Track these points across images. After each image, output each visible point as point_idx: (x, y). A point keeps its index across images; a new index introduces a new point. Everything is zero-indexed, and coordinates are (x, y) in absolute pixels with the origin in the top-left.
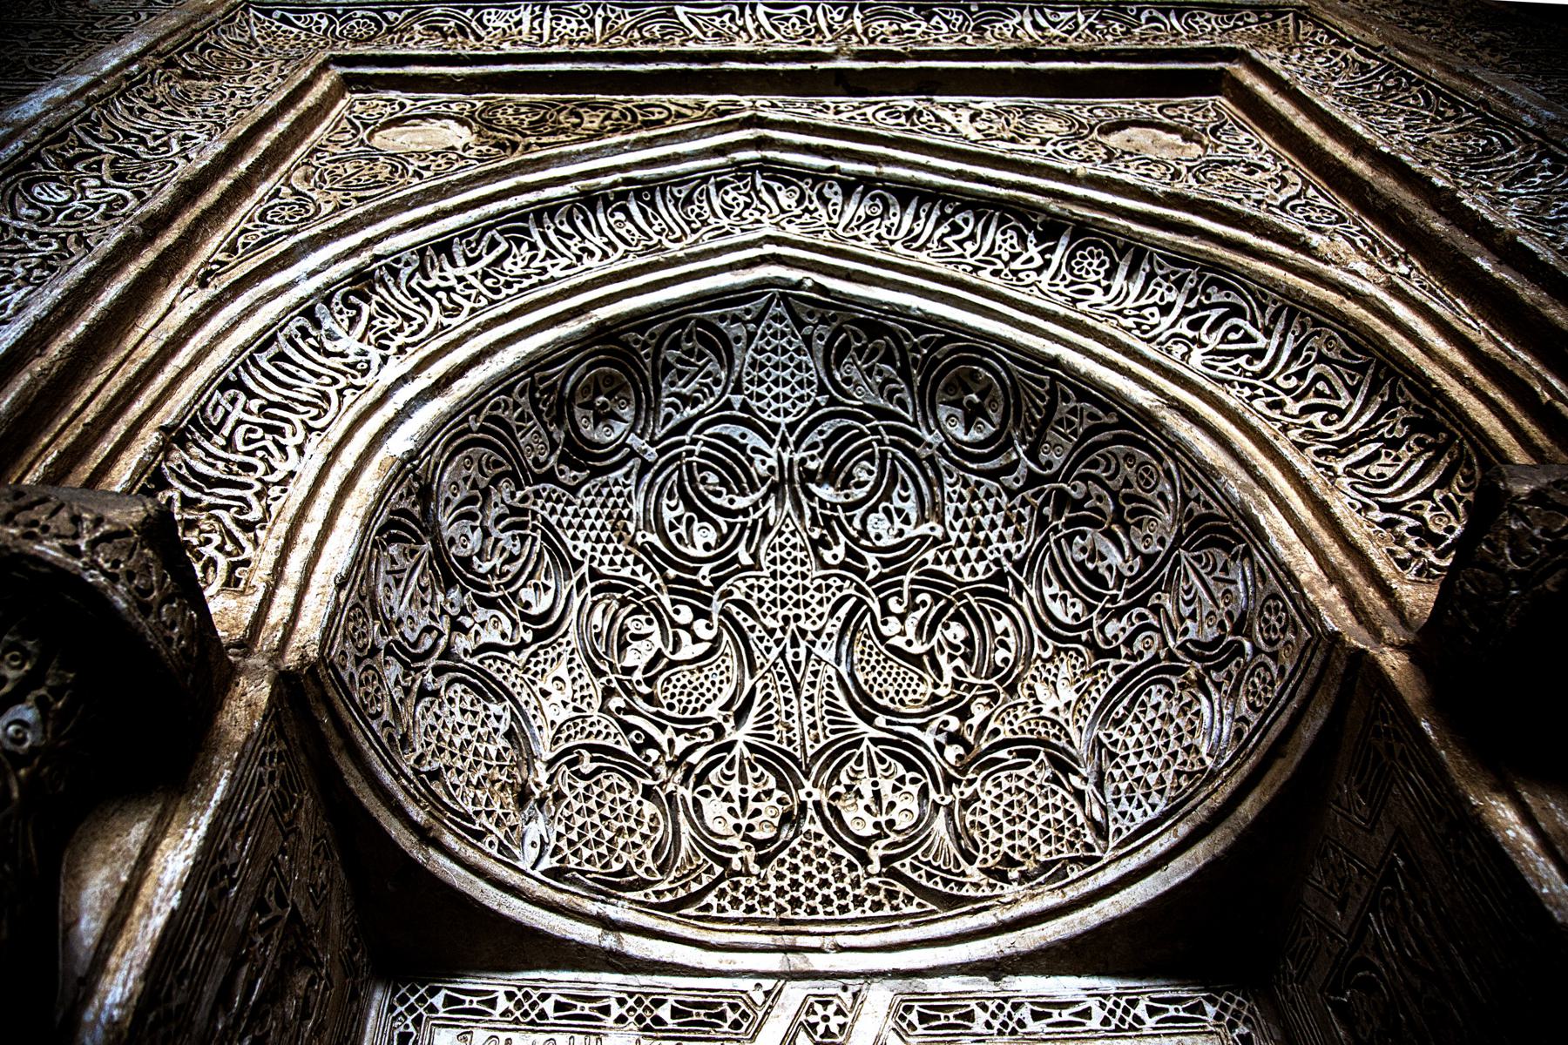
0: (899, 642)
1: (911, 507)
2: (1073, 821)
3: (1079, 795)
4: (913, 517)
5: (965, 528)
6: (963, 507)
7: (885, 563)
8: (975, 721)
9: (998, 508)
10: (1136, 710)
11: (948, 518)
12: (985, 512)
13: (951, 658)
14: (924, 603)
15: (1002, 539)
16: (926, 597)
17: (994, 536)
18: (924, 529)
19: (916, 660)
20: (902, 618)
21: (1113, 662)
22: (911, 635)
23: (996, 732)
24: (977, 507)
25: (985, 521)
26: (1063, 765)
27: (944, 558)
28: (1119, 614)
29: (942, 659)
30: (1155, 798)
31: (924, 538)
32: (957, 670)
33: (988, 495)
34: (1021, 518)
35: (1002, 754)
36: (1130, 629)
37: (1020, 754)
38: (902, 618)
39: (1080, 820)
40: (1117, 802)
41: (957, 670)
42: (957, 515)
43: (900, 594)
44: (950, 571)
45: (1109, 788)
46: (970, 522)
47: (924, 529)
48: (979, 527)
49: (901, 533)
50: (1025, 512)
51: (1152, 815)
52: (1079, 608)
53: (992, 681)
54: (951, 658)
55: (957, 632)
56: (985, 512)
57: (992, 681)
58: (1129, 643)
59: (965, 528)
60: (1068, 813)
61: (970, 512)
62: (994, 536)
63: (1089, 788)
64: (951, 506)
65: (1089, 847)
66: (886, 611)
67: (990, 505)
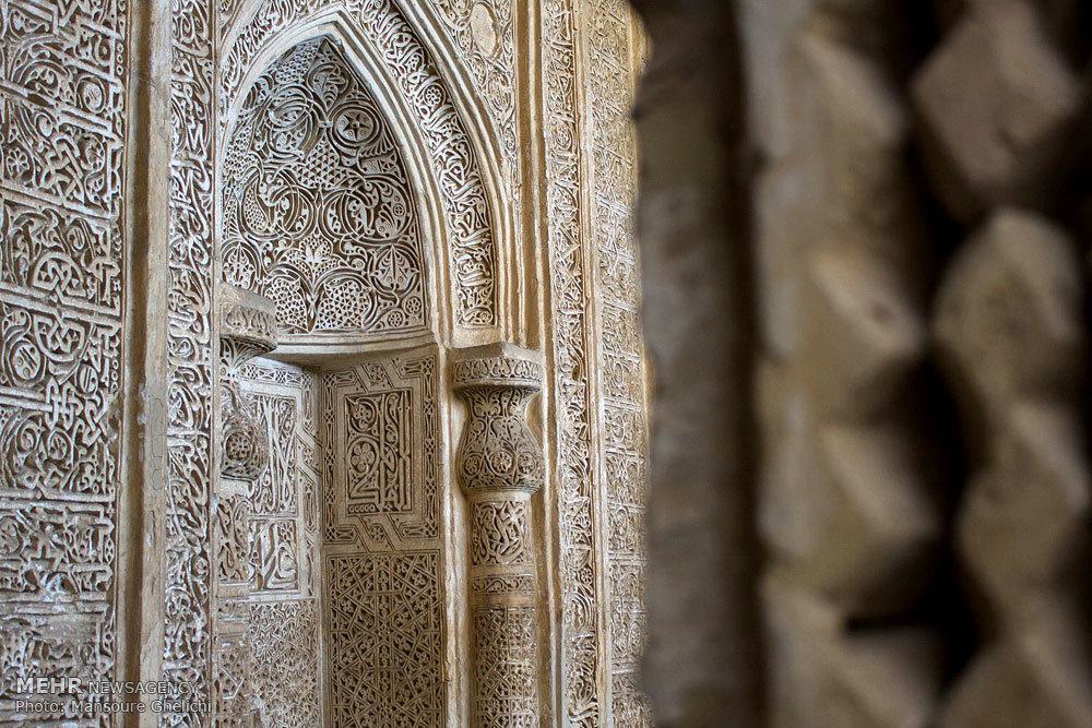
0: (263, 197)
1: (299, 140)
2: (302, 314)
3: (308, 305)
4: (297, 145)
5: (314, 163)
6: (319, 155)
7: (274, 157)
8: (279, 250)
9: (332, 165)
10: (343, 285)
11: (310, 155)
12: (326, 162)
13: (279, 215)
14: (280, 184)
15: (325, 177)
16: (282, 182)
17: (323, 174)
18: (298, 152)
19: (265, 208)
20: (269, 186)
21: (342, 260)
22: (269, 196)
23: (285, 259)
24: (325, 158)
25: (324, 166)
26: (305, 289)
27: (298, 169)
28: (354, 244)
29: (276, 213)
30: (336, 323)
31: (295, 156)
32: (279, 221)
33: (332, 157)
34: (338, 176)
35: (284, 270)
36: (355, 253)
37: (290, 273)
38: (269, 186)
39: (305, 314)
40: (321, 315)
41: (279, 221)
42: (315, 156)
43: (273, 175)
44: (297, 176)
45: (320, 309)
46: (318, 162)
47: (298, 152)
48: (319, 166)
49: (288, 148)
50: (342, 176)
51: (332, 328)
52: (339, 228)
53: (290, 234)
54: (279, 215)
55: (286, 204)
56: (326, 162)
57: (290, 234)
58: (352, 257)
59: (314, 163)
60: (301, 309)
61: (320, 158)
62: (323, 174)
63: (313, 304)
64: (315, 151)
65: (304, 326)
66: (264, 180)
67: (330, 162)
